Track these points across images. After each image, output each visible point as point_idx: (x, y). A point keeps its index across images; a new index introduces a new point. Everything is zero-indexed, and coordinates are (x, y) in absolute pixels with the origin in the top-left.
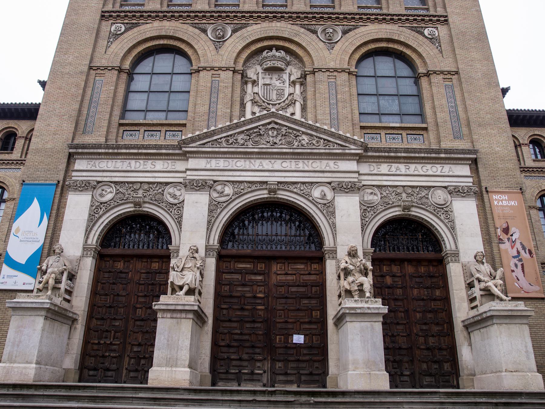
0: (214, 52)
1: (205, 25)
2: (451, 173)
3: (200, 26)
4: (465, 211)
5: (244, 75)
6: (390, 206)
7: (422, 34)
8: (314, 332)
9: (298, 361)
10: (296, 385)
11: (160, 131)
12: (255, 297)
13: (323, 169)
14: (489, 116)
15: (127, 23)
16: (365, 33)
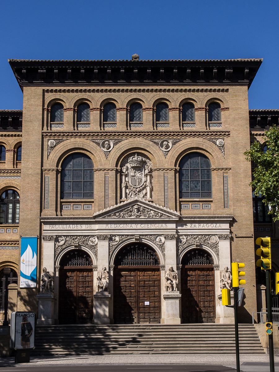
0: (105, 159)
1: (99, 140)
2: (220, 228)
3: (96, 141)
4: (224, 245)
5: (121, 172)
6: (190, 244)
7: (215, 143)
8: (156, 300)
9: (149, 313)
10: (148, 322)
11: (81, 205)
12: (131, 286)
13: (160, 228)
14: (243, 196)
15: (56, 139)
16: (185, 144)
